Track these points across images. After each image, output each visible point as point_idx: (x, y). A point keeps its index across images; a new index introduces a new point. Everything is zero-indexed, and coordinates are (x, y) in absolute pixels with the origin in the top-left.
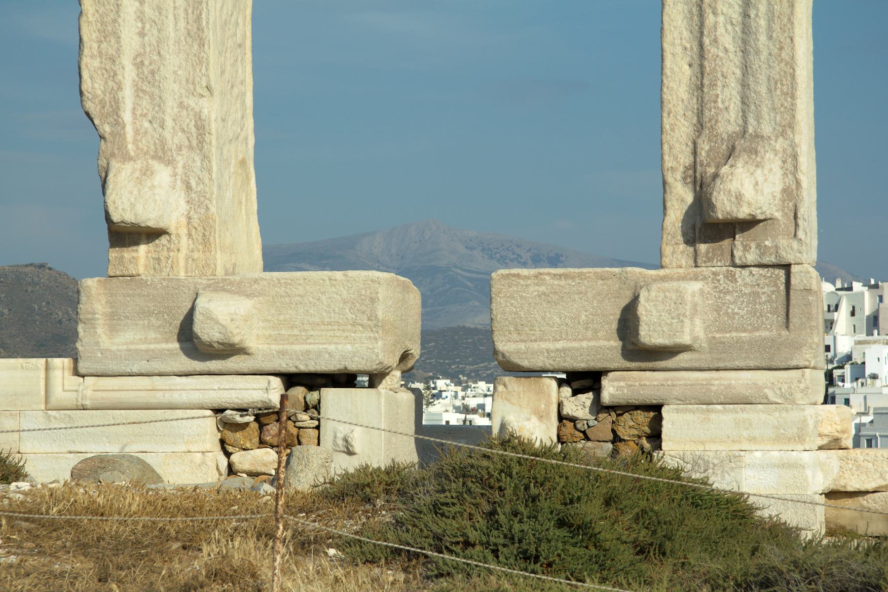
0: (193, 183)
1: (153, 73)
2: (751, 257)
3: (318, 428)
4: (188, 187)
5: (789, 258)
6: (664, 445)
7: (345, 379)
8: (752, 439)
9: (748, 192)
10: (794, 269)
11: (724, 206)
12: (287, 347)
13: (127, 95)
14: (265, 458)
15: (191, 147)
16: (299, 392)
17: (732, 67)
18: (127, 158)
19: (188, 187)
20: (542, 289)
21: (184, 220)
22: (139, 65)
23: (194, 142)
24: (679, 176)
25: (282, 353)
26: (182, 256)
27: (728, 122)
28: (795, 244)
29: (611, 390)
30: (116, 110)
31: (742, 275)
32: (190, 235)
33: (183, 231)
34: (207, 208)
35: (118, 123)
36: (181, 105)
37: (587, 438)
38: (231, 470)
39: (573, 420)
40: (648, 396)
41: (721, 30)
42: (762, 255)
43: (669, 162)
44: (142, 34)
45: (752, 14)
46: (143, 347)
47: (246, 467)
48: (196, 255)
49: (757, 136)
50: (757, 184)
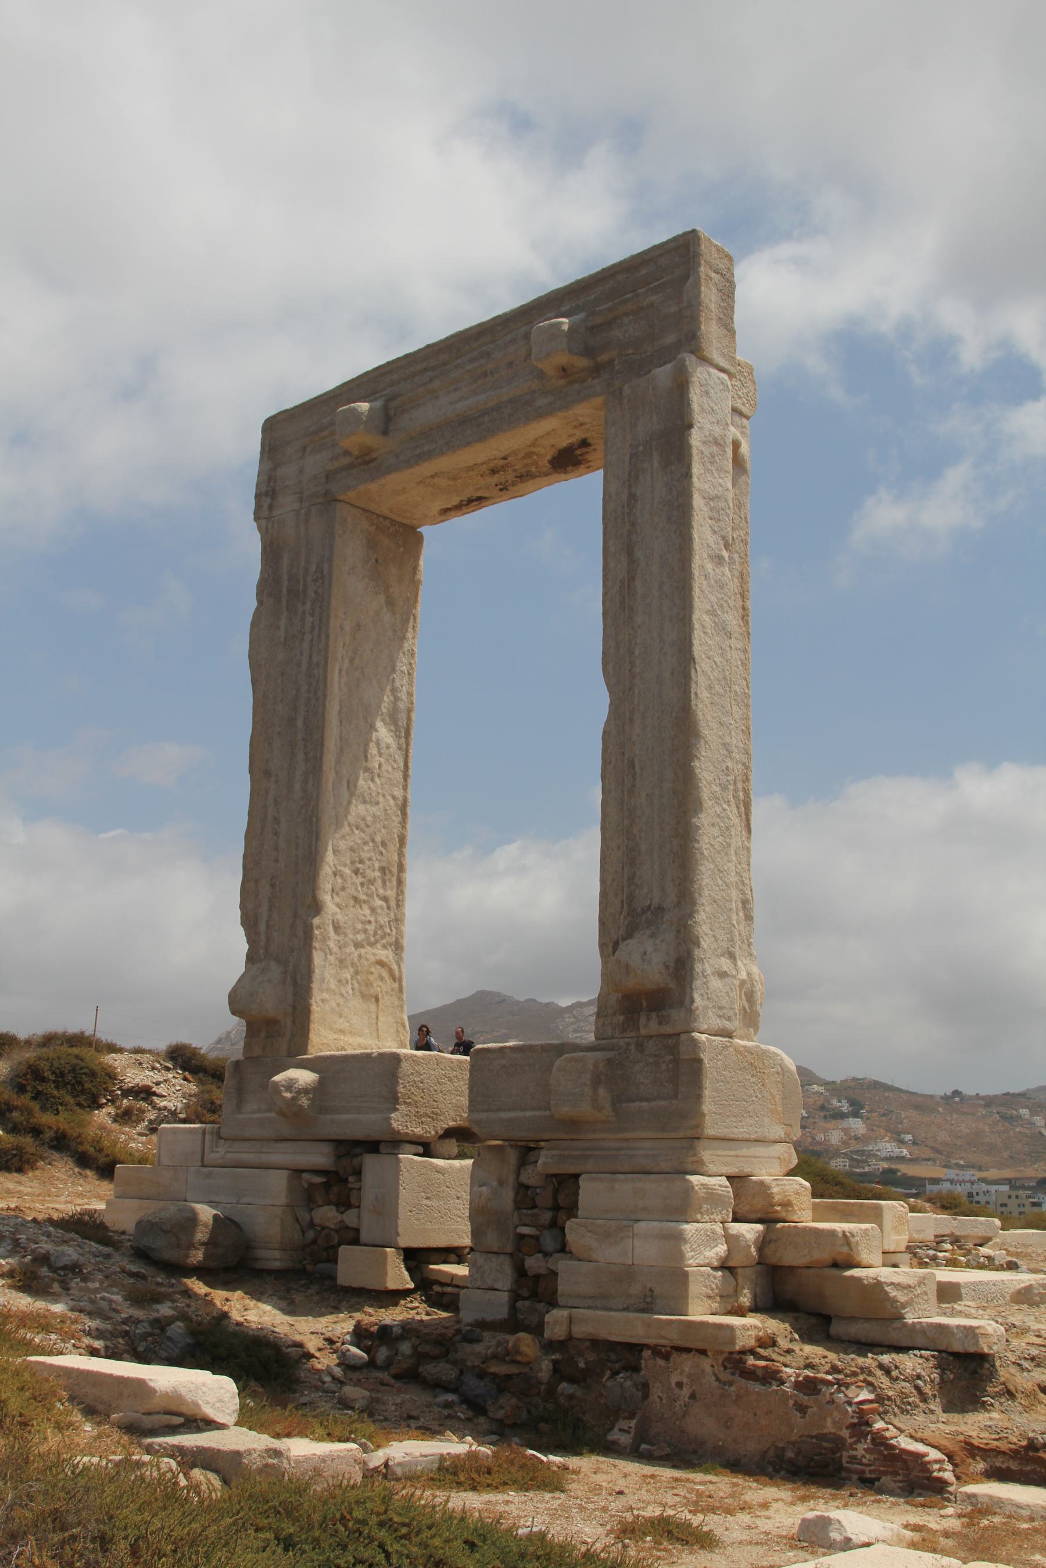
3: (360, 1189)
10: (683, 1037)
20: (504, 1062)
33: (289, 1021)
36: (295, 915)
42: (660, 1023)
49: (660, 909)
50: (645, 953)
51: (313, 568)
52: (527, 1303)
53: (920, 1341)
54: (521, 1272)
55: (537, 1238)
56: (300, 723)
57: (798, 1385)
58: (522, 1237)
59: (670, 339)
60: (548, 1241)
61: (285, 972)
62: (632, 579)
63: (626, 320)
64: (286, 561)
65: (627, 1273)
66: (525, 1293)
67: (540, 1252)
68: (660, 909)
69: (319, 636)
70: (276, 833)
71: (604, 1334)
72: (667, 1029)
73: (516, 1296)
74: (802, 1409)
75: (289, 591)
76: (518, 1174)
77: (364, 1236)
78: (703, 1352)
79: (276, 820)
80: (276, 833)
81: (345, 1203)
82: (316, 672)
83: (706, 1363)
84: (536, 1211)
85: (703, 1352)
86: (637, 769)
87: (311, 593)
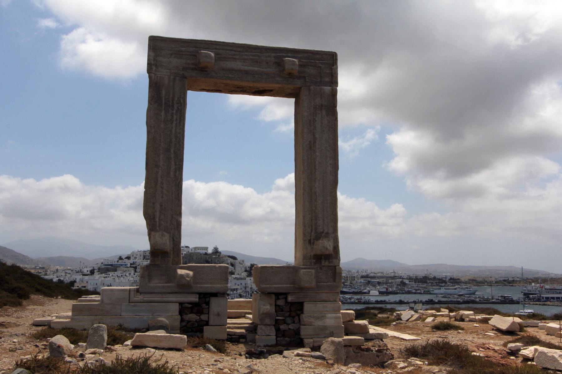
3: (209, 308)
4: (173, 240)
8: (327, 311)
9: (329, 248)
13: (158, 214)
14: (192, 317)
19: (173, 240)
22: (161, 206)
25: (201, 287)
29: (290, 299)
30: (154, 218)
32: (173, 253)
33: (172, 252)
36: (172, 217)
37: (282, 311)
38: (182, 320)
39: (279, 306)
47: (187, 319)
49: (327, 233)
51: (176, 99)
52: (282, 338)
53: (374, 337)
54: (278, 330)
55: (283, 320)
56: (172, 152)
57: (376, 351)
58: (276, 320)
59: (327, 79)
60: (289, 320)
61: (170, 236)
62: (315, 142)
63: (310, 67)
64: (164, 92)
66: (280, 335)
67: (285, 323)
68: (327, 233)
69: (180, 123)
70: (162, 188)
72: (331, 265)
73: (277, 336)
74: (378, 356)
76: (275, 302)
77: (211, 323)
78: (350, 346)
79: (162, 183)
80: (162, 188)
81: (200, 312)
83: (351, 349)
85: (350, 346)
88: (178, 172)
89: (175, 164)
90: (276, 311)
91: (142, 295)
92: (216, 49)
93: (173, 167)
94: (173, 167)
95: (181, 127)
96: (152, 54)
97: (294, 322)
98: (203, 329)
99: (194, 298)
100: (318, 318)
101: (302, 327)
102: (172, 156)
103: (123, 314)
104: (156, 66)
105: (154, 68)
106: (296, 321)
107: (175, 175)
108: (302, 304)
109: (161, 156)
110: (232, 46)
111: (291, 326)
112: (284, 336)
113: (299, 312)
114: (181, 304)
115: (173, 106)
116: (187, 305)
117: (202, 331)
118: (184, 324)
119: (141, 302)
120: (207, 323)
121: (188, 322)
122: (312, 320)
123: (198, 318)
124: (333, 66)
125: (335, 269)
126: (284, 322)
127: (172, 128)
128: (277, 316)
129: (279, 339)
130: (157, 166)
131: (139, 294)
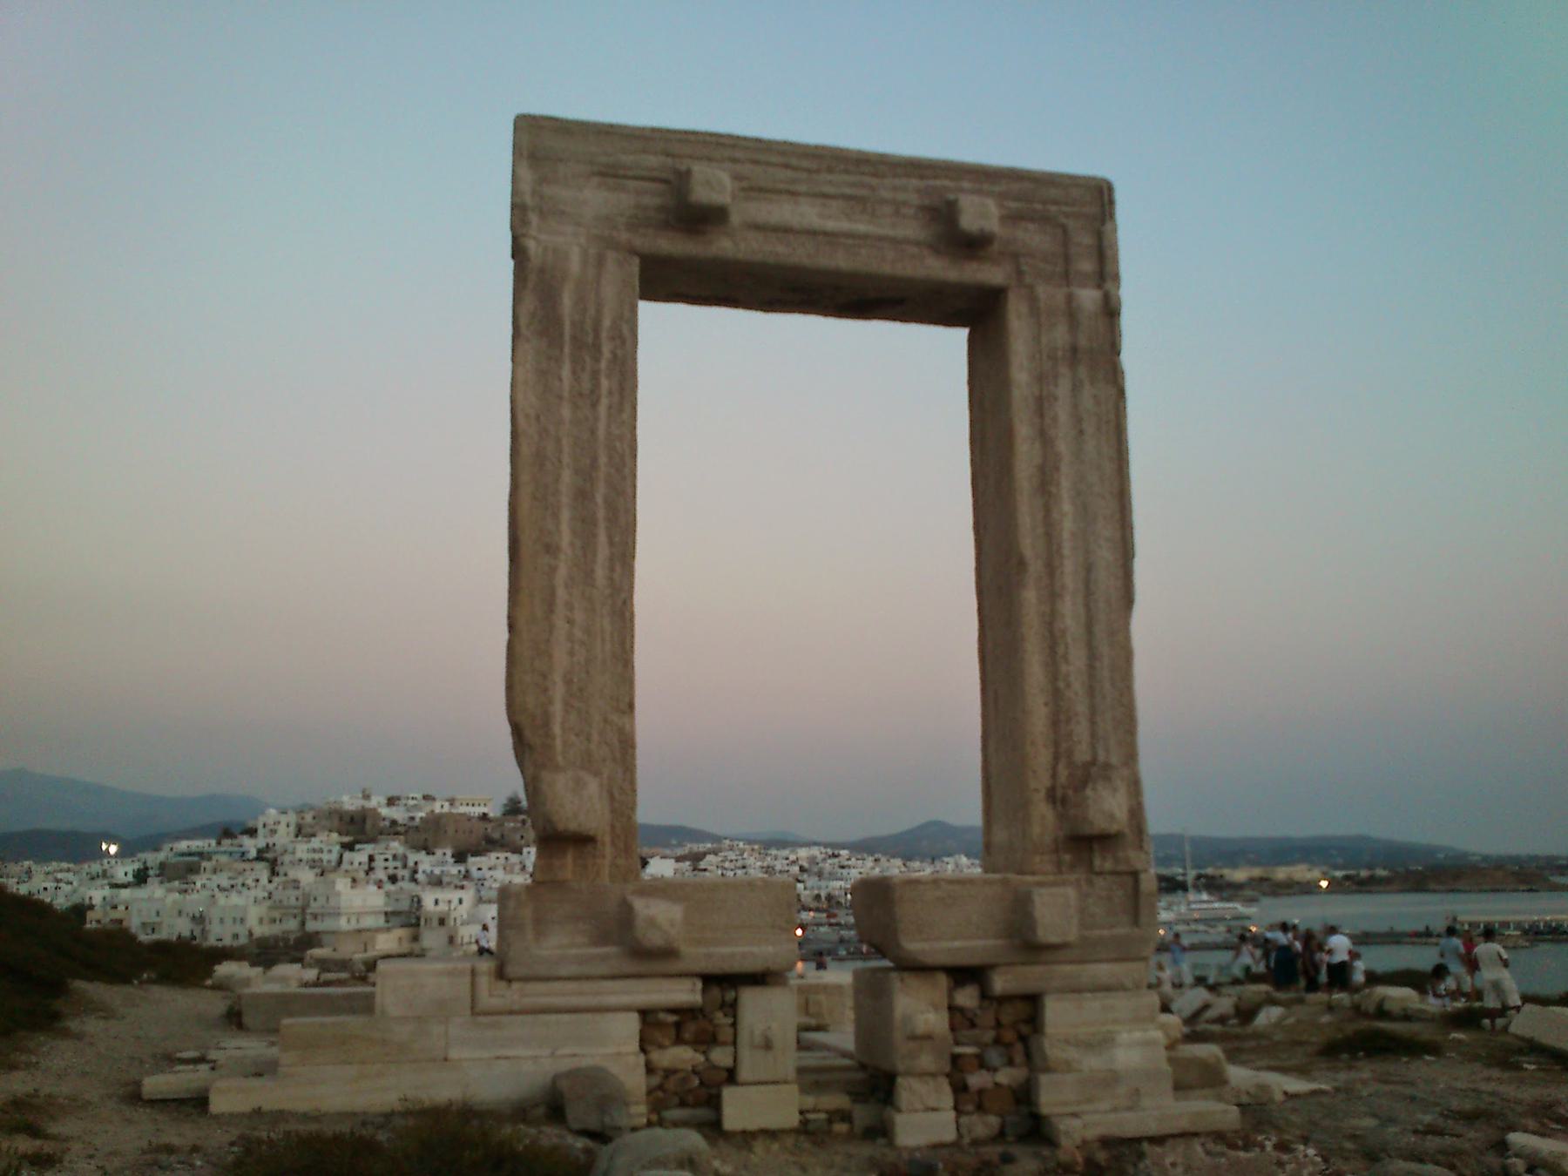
0: (617, 795)
1: (581, 690)
2: (1108, 865)
3: (734, 1025)
4: (612, 798)
5: (1139, 866)
6: (1049, 1029)
7: (760, 979)
8: (1116, 1021)
10: (1143, 876)
11: (1100, 824)
12: (712, 949)
13: (557, 708)
14: (682, 1056)
15: (614, 760)
16: (715, 992)
17: (1081, 708)
18: (557, 769)
21: (608, 829)
22: (568, 682)
23: (618, 755)
24: (1042, 794)
26: (607, 862)
27: (1082, 754)
28: (1143, 856)
30: (547, 723)
31: (1100, 882)
32: (613, 843)
33: (607, 839)
34: (630, 818)
35: (548, 735)
36: (605, 721)
37: (973, 1025)
38: (650, 1069)
40: (1030, 986)
41: (1072, 678)
43: (1033, 784)
44: (571, 653)
45: (1098, 664)
46: (574, 951)
48: (621, 861)
52: (974, 1117)
54: (960, 1089)
58: (955, 1059)
60: (994, 1057)
63: (1031, 226)
64: (567, 301)
65: (1111, 1079)
66: (970, 1108)
71: (1117, 1132)
72: (1122, 868)
74: (1280, 1164)
75: (574, 338)
76: (950, 997)
77: (744, 1073)
79: (570, 606)
80: (570, 621)
81: (706, 1040)
82: (618, 444)
84: (977, 1032)
85: (1196, 1134)
86: (1069, 640)
87: (606, 350)
88: (618, 568)
89: (611, 543)
90: (953, 1028)
91: (516, 986)
92: (734, 160)
93: (603, 551)
94: (603, 551)
95: (625, 416)
96: (527, 174)
97: (1010, 1063)
98: (718, 1097)
99: (686, 993)
100: (1088, 1045)
101: (1044, 1079)
102: (601, 514)
103: (454, 1054)
104: (542, 214)
105: (534, 218)
106: (1019, 1057)
107: (611, 579)
108: (1033, 1002)
109: (565, 515)
110: (783, 153)
111: (1005, 1076)
112: (980, 1108)
113: (1025, 1029)
114: (645, 1014)
115: (597, 347)
116: (662, 1016)
117: (714, 1102)
118: (656, 1080)
119: (511, 1012)
120: (731, 1076)
121: (669, 1072)
122: (1072, 1053)
123: (701, 1058)
124: (1103, 222)
125: (1136, 881)
126: (982, 1063)
127: (596, 419)
128: (957, 1043)
129: (964, 1120)
130: (551, 549)
131: (503, 984)
